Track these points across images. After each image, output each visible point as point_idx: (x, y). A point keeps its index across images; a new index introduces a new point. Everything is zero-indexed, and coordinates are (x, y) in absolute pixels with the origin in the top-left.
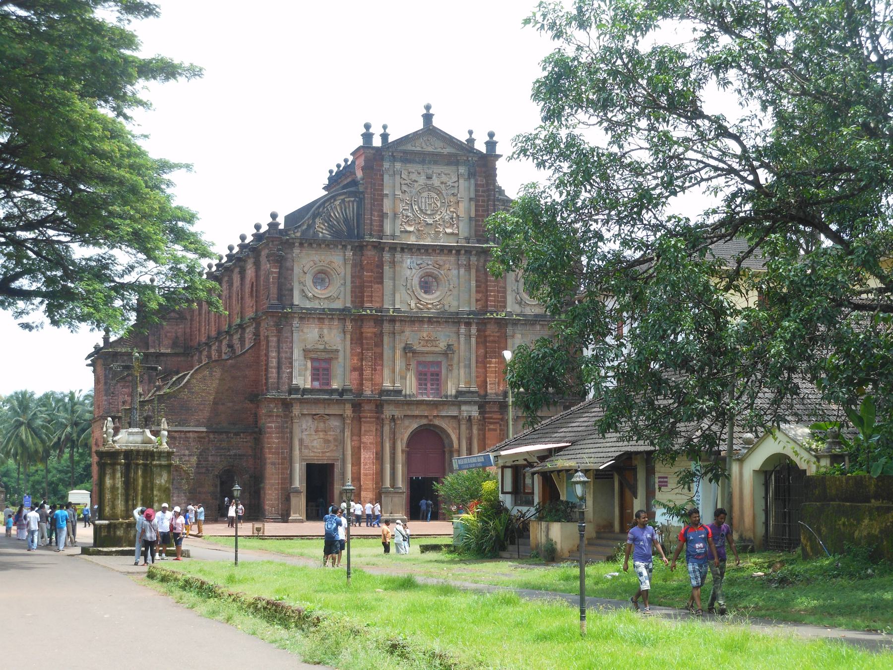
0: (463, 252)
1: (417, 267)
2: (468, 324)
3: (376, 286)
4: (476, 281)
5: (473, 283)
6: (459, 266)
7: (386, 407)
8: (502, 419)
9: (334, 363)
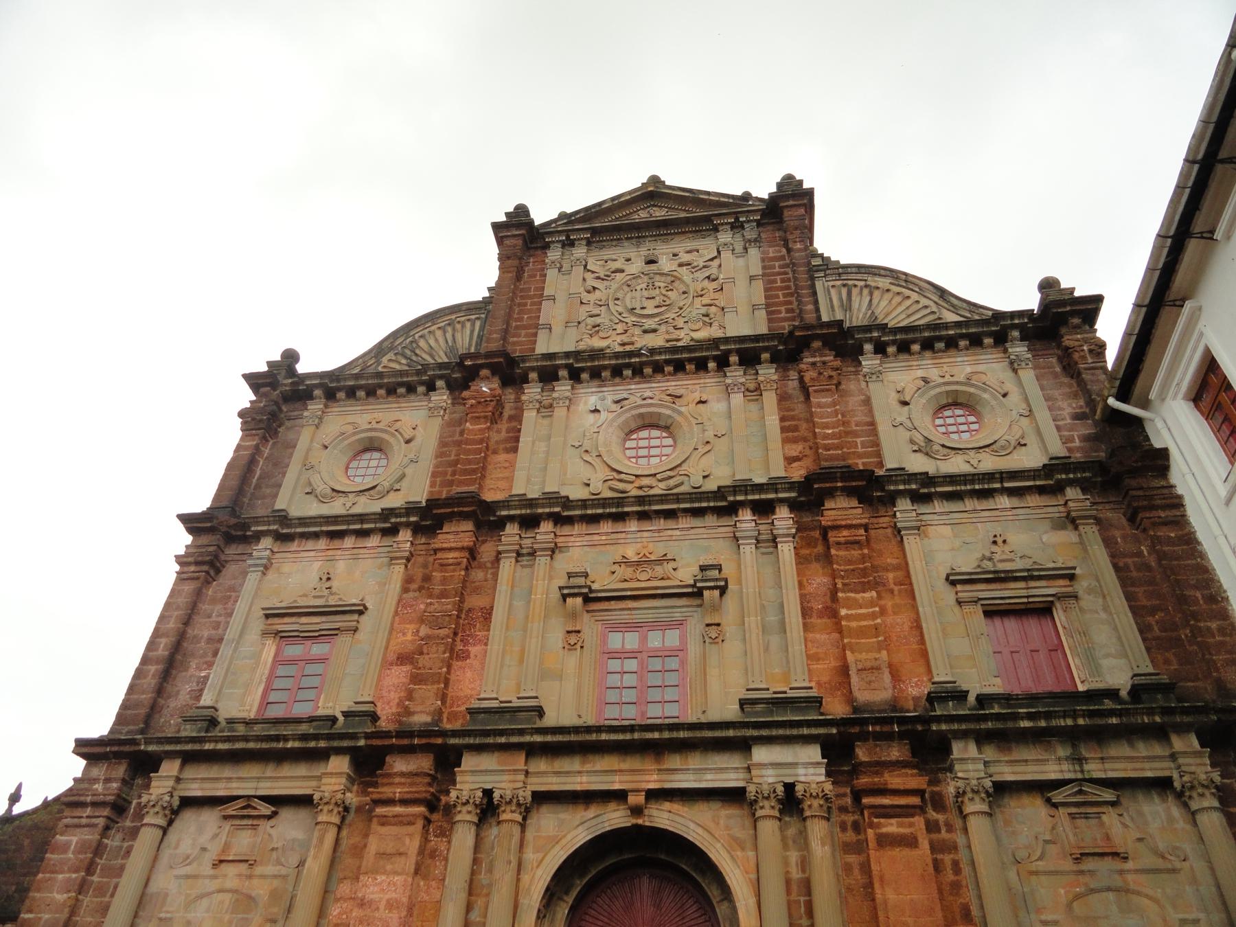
0: (734, 359)
1: (614, 407)
2: (764, 509)
3: (502, 457)
4: (782, 419)
5: (773, 421)
6: (728, 390)
7: (469, 762)
8: (938, 803)
9: (343, 640)
